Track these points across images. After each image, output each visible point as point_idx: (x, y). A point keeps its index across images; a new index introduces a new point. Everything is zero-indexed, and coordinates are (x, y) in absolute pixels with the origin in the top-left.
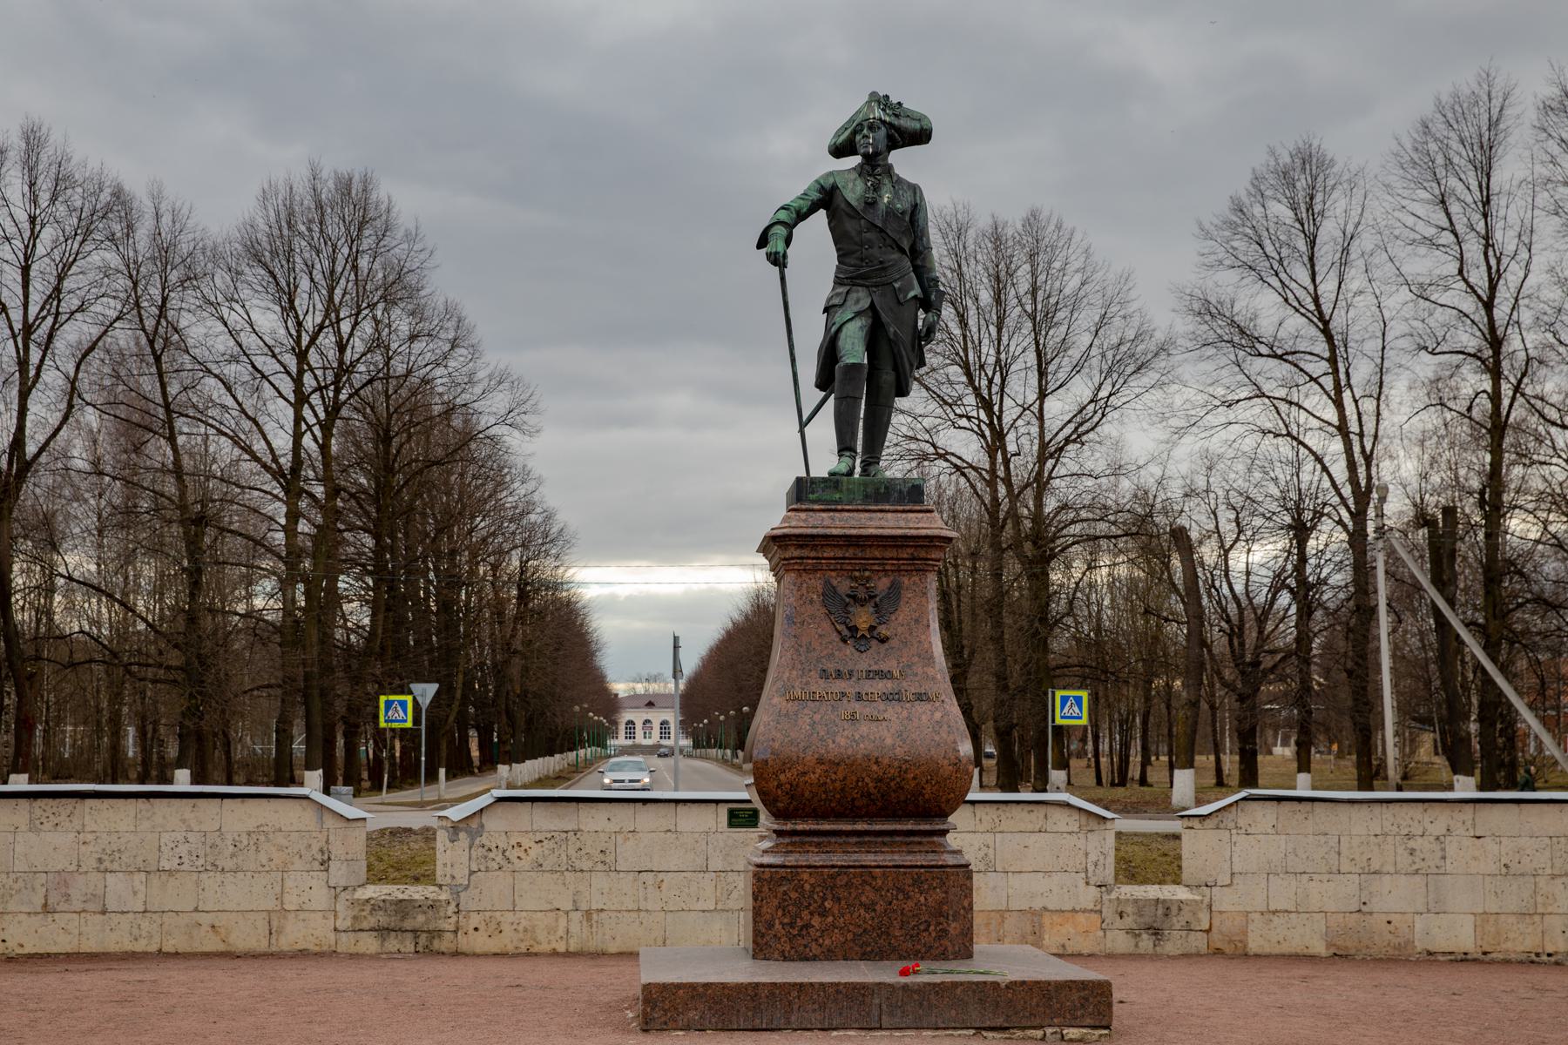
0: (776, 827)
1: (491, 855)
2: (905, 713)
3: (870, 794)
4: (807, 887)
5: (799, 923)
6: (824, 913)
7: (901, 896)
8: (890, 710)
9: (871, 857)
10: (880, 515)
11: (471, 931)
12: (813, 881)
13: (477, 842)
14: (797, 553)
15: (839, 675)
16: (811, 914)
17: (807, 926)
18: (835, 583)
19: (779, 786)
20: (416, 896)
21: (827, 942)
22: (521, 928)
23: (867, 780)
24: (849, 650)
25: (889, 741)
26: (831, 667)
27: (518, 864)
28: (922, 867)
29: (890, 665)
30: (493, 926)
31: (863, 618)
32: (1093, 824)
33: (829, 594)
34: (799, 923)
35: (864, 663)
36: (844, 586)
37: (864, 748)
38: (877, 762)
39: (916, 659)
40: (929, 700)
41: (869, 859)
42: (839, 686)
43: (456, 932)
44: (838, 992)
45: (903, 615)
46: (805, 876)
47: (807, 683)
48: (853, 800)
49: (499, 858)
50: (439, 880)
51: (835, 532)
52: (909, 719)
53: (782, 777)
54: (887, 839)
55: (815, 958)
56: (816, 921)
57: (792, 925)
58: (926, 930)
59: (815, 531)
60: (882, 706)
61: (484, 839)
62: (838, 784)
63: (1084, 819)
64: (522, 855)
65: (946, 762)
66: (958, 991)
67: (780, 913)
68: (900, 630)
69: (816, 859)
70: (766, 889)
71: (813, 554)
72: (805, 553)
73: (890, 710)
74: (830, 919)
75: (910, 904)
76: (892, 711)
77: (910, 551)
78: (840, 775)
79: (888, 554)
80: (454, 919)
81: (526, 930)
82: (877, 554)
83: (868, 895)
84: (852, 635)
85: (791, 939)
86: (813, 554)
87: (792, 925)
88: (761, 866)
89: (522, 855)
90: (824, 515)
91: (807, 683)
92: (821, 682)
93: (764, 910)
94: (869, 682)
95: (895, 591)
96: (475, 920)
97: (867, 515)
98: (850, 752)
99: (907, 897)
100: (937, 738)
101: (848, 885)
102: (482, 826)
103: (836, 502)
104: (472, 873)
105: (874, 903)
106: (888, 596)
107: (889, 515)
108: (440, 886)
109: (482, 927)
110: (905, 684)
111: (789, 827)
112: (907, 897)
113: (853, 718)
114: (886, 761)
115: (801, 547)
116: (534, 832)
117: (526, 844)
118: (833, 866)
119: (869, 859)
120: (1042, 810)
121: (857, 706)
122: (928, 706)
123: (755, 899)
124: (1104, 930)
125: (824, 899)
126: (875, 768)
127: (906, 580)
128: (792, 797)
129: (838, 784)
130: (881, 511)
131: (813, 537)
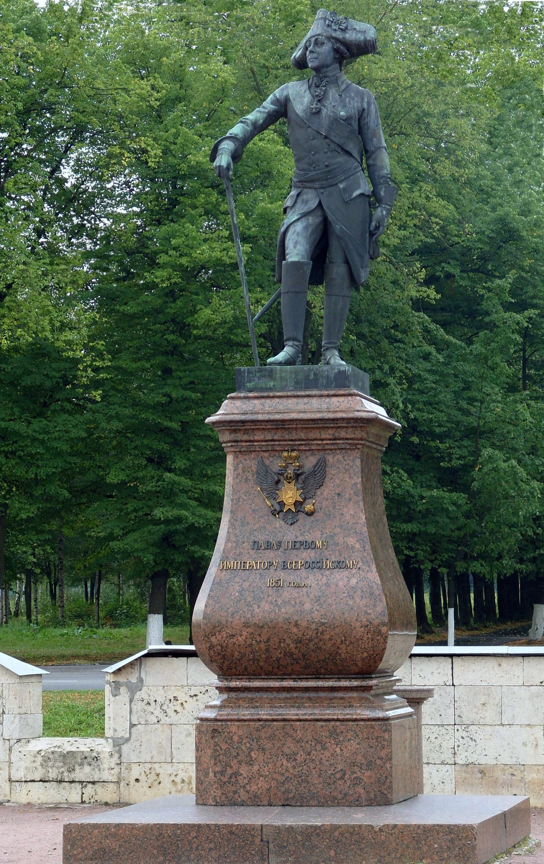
0: (220, 684)
1: (150, 709)
2: (324, 579)
3: (292, 654)
4: (236, 738)
5: (229, 771)
6: (250, 762)
7: (319, 747)
8: (311, 577)
9: (294, 711)
10: (306, 400)
11: (133, 782)
12: (241, 733)
13: (138, 695)
14: (232, 437)
15: (269, 546)
16: (240, 763)
17: (236, 774)
18: (267, 462)
19: (211, 647)
20: (83, 748)
21: (254, 788)
22: (178, 780)
23: (287, 641)
24: (278, 523)
25: (307, 606)
26: (261, 538)
27: (174, 718)
28: (338, 720)
30: (153, 777)
33: (263, 474)
34: (229, 771)
35: (291, 534)
36: (277, 464)
37: (287, 611)
38: (296, 625)
39: (339, 530)
40: (346, 567)
41: (292, 713)
42: (269, 555)
43: (118, 783)
44: (231, 833)
45: (327, 491)
46: (234, 729)
47: (241, 554)
48: (278, 660)
49: (158, 712)
50: (107, 735)
51: (260, 417)
52: (327, 585)
53: (213, 640)
54: (312, 695)
55: (243, 804)
56: (244, 770)
57: (222, 773)
58: (342, 778)
59: (243, 417)
60: (303, 573)
61: (142, 694)
62: (262, 645)
64: (179, 708)
65: (358, 624)
66: (336, 834)
68: (324, 503)
69: (246, 713)
70: (203, 741)
71: (246, 437)
72: (239, 436)
73: (311, 577)
74: (256, 768)
75: (327, 754)
76: (313, 579)
77: (331, 431)
78: (264, 638)
79: (312, 435)
80: (116, 770)
81: (183, 781)
82: (302, 435)
83: (290, 747)
84: (279, 510)
85: (222, 785)
86: (246, 437)
87: (222, 773)
88: (202, 719)
89: (179, 708)
90: (256, 402)
91: (241, 554)
92: (252, 552)
93: (203, 759)
94: (295, 552)
95: (321, 469)
96: (136, 771)
97: (294, 400)
98: (272, 616)
100: (351, 603)
101: (272, 737)
102: (141, 680)
103: (271, 389)
104: (132, 726)
106: (313, 473)
107: (314, 401)
108: (107, 738)
109: (143, 778)
110: (327, 553)
111: (234, 684)
113: (277, 585)
114: (304, 624)
115: (235, 431)
116: (190, 686)
117: (182, 698)
118: (259, 720)
119: (292, 713)
121: (282, 575)
122: (346, 573)
123: (197, 750)
126: (295, 630)
127: (330, 459)
128: (224, 657)
129: (262, 645)
130: (309, 396)
131: (243, 422)
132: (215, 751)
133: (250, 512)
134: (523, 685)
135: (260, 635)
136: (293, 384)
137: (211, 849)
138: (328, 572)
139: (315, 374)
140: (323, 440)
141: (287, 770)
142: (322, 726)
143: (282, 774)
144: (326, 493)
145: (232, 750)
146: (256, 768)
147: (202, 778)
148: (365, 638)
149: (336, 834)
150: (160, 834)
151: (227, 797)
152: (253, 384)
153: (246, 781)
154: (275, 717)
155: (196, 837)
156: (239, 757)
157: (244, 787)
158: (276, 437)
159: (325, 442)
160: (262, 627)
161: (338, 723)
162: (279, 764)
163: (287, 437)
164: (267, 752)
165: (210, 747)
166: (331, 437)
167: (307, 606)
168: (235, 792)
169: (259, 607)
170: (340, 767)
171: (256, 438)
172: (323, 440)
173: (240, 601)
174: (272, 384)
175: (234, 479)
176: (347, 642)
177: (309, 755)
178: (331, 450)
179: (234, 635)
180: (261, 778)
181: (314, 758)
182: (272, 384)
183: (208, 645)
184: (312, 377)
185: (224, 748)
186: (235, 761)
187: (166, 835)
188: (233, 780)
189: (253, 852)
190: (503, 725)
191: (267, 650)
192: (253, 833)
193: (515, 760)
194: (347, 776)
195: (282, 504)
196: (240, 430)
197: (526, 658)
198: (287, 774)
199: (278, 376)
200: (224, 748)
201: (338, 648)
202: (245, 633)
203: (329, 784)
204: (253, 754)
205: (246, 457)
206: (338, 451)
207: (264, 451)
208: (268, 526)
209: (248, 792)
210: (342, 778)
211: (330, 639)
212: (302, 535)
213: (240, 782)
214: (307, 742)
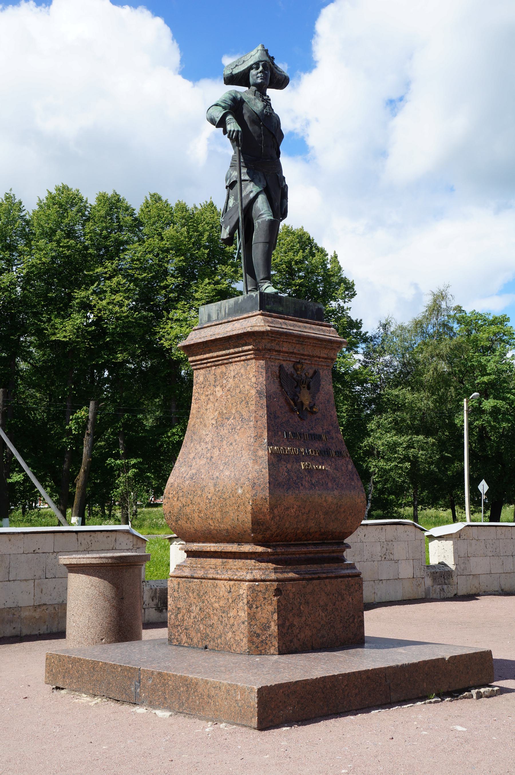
4: (291, 595)
5: (287, 624)
6: (300, 614)
7: (340, 598)
17: (292, 625)
23: (320, 513)
29: (319, 430)
31: (305, 398)
32: (140, 543)
34: (287, 624)
39: (331, 428)
44: (368, 678)
46: (289, 587)
56: (296, 621)
63: (135, 539)
65: (359, 501)
67: (275, 616)
71: (277, 348)
74: (304, 619)
77: (326, 351)
93: (259, 615)
99: (343, 599)
105: (326, 605)
112: (343, 599)
120: (114, 535)
124: (144, 609)
125: (301, 604)
129: (305, 516)
132: (278, 606)
133: (279, 408)
134: (23, 553)
135: (304, 508)
136: (293, 312)
137: (356, 694)
138: (333, 459)
139: (305, 307)
140: (319, 357)
141: (322, 619)
142: (341, 581)
143: (319, 623)
144: (320, 398)
145: (288, 605)
146: (304, 619)
147: (258, 631)
148: (362, 511)
149: (426, 668)
150: (325, 686)
151: (286, 646)
152: (270, 306)
153: (297, 631)
154: (313, 576)
155: (347, 685)
156: (293, 611)
157: (297, 636)
158: (295, 351)
159: (321, 360)
160: (306, 501)
161: (350, 579)
162: (317, 614)
163: (301, 352)
164: (310, 605)
165: (271, 604)
166: (325, 356)
167: (330, 485)
168: (291, 641)
169: (302, 485)
170: (352, 613)
171: (284, 349)
172: (319, 357)
173: (289, 479)
174: (281, 309)
175: (266, 380)
176: (353, 514)
177: (334, 605)
178: (322, 365)
179: (288, 508)
180: (307, 628)
181: (337, 607)
182: (281, 309)
183: (272, 516)
184: (303, 309)
185: (284, 604)
186: (291, 615)
187: (328, 687)
188: (290, 631)
189: (381, 693)
190: (9, 581)
191: (307, 520)
192: (380, 676)
193: (15, 604)
194: (356, 620)
195: (302, 404)
196: (275, 340)
197: (26, 535)
198: (322, 622)
199: (284, 303)
200: (284, 604)
201: (347, 519)
202: (295, 506)
203: (346, 628)
204: (301, 608)
205: (273, 364)
206: (325, 367)
207: (284, 360)
208: (290, 420)
209: (299, 640)
210: (353, 622)
211: (344, 512)
212: (312, 429)
213: (294, 632)
214: (333, 595)
